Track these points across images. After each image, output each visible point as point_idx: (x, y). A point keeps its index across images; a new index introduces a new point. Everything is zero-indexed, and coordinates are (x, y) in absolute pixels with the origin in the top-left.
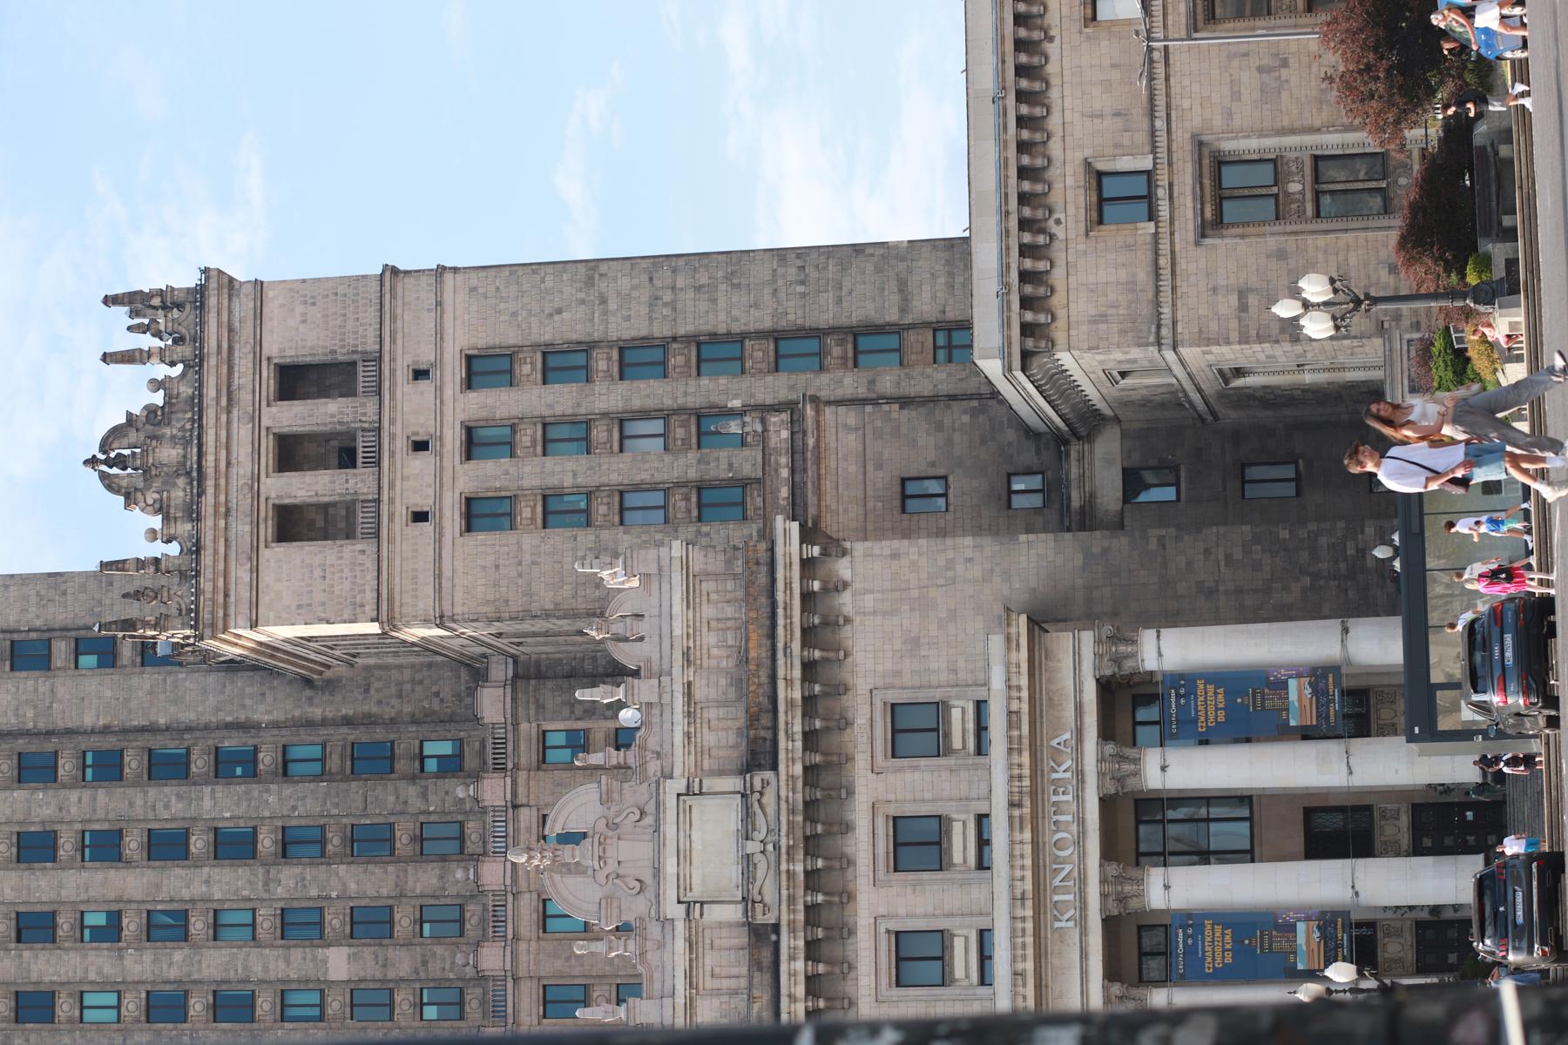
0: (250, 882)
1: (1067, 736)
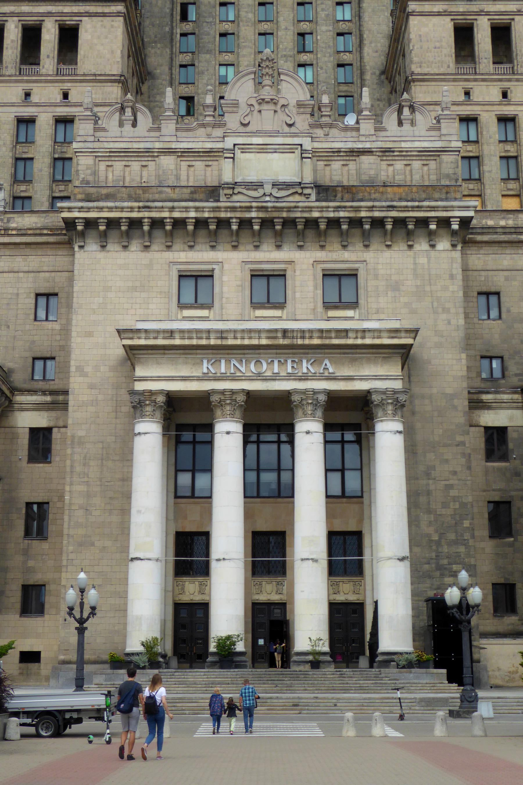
0: (286, 48)
1: (331, 370)
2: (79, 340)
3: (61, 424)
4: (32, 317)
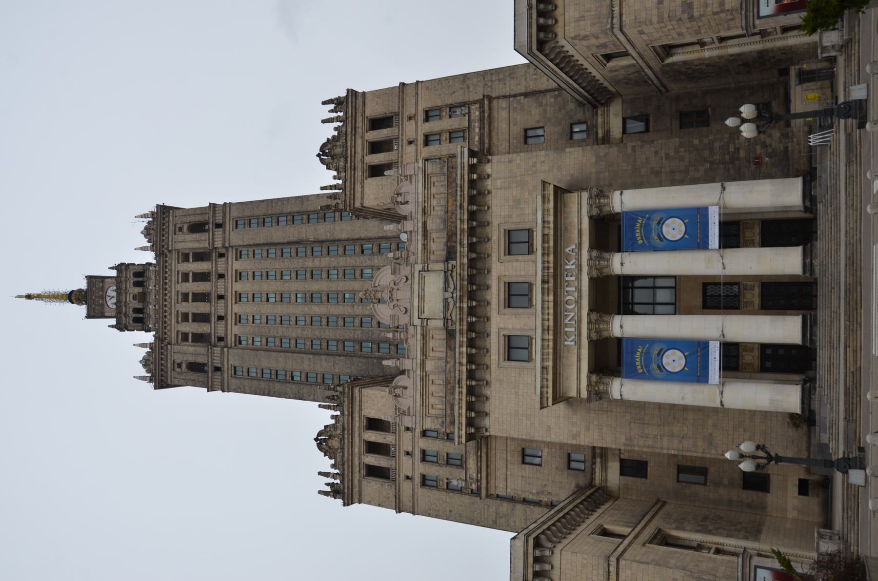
1: (574, 247)
2: (553, 436)
3: (618, 452)
4: (539, 468)
